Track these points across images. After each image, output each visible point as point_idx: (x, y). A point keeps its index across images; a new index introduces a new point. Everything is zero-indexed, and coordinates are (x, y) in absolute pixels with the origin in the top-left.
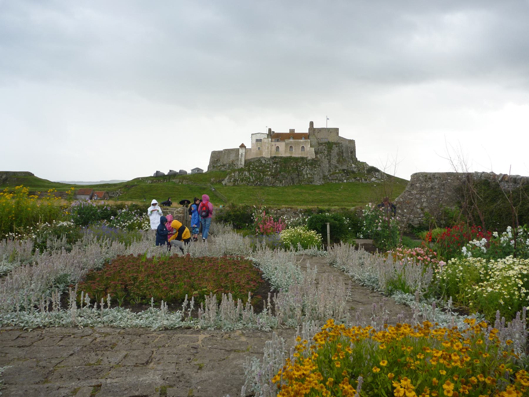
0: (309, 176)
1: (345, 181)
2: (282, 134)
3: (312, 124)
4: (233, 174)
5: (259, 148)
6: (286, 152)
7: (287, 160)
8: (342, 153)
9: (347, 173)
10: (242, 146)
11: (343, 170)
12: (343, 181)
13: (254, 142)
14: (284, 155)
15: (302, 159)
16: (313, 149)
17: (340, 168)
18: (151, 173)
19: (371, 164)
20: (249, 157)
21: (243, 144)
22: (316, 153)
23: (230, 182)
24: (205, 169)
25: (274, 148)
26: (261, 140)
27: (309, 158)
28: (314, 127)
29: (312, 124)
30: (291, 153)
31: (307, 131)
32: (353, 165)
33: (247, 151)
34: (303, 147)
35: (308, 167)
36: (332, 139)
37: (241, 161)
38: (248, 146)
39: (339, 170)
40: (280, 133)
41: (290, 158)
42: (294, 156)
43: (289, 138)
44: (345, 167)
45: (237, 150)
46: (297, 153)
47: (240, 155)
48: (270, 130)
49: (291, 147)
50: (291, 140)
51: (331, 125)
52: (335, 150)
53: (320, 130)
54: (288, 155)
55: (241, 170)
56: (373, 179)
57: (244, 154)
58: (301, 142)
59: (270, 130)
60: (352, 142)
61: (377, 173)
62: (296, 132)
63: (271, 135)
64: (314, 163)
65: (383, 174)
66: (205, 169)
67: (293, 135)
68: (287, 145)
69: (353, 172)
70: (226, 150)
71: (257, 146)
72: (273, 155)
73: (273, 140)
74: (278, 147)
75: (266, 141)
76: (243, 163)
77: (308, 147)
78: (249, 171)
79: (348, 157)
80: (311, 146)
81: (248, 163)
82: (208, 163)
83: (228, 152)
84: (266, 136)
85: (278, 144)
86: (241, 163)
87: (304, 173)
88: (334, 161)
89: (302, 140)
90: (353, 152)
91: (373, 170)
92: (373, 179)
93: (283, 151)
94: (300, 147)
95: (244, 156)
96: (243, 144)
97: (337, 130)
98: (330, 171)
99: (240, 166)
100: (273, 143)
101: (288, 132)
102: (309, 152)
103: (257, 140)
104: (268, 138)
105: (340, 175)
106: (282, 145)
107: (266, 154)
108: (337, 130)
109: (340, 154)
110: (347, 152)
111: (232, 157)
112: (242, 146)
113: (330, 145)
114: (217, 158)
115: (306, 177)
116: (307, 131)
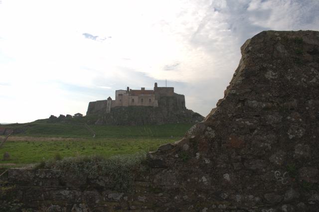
1: (178, 122)
3: (156, 84)
10: (109, 99)
11: (177, 115)
13: (117, 96)
14: (137, 105)
15: (150, 107)
16: (157, 101)
18: (47, 117)
22: (159, 103)
24: (84, 114)
25: (131, 100)
28: (158, 86)
29: (156, 84)
32: (183, 112)
38: (114, 98)
42: (143, 105)
45: (104, 102)
46: (146, 104)
47: (108, 105)
48: (128, 88)
49: (142, 100)
54: (140, 104)
57: (110, 104)
59: (128, 88)
60: (183, 96)
61: (199, 117)
62: (146, 89)
66: (84, 114)
74: (133, 100)
76: (110, 109)
77: (153, 100)
82: (86, 110)
84: (125, 92)
85: (133, 97)
90: (183, 102)
93: (137, 102)
97: (172, 89)
99: (108, 112)
100: (130, 97)
101: (140, 89)
102: (155, 104)
103: (119, 95)
104: (127, 93)
106: (136, 98)
107: (125, 104)
108: (172, 89)
112: (109, 99)
114: (92, 105)
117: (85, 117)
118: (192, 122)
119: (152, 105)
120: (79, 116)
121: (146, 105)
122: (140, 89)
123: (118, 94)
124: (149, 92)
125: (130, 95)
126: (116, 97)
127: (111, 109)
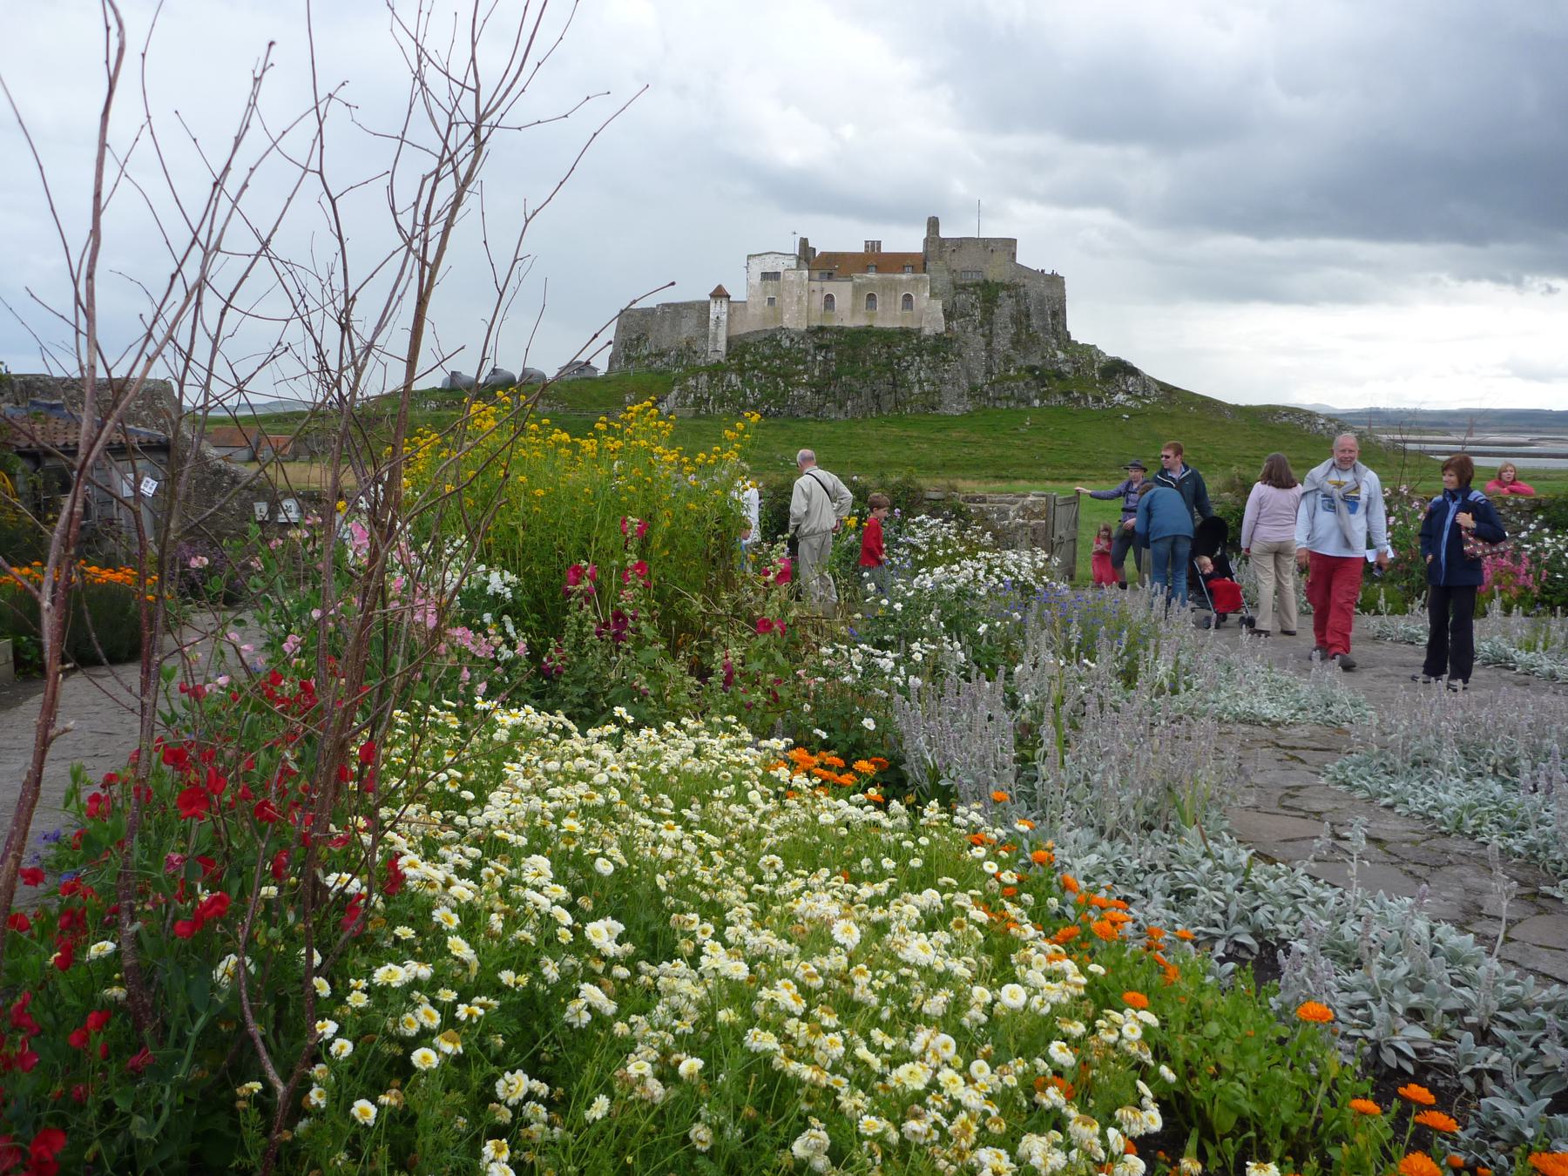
0: (926, 387)
1: (1037, 403)
2: (843, 254)
4: (692, 382)
5: (771, 301)
6: (854, 311)
7: (858, 339)
8: (1028, 316)
9: (1043, 377)
10: (719, 294)
11: (1031, 370)
12: (1028, 402)
13: (756, 279)
14: (849, 323)
15: (906, 333)
16: (938, 305)
17: (1021, 362)
19: (1111, 348)
20: (741, 329)
21: (720, 287)
22: (949, 316)
23: (684, 405)
24: (601, 365)
25: (818, 301)
26: (775, 276)
27: (927, 331)
28: (943, 234)
29: (933, 224)
30: (871, 317)
31: (918, 247)
32: (1060, 355)
33: (735, 308)
34: (908, 298)
35: (922, 361)
36: (994, 273)
37: (715, 340)
38: (738, 293)
39: (1019, 370)
40: (836, 254)
41: (868, 332)
43: (866, 269)
44: (1035, 361)
45: (704, 308)
46: (889, 317)
47: (711, 324)
48: (804, 242)
49: (871, 297)
50: (872, 275)
51: (993, 230)
52: (1006, 308)
53: (960, 243)
54: (860, 321)
55: (715, 370)
56: (1120, 397)
57: (724, 317)
58: (901, 281)
59: (804, 242)
60: (1056, 281)
61: (1131, 379)
63: (807, 261)
64: (941, 347)
65: (1146, 383)
66: (601, 365)
67: (874, 259)
68: (857, 290)
69: (1060, 375)
70: (668, 305)
71: (766, 293)
72: (816, 324)
73: (816, 275)
74: (829, 298)
75: (792, 276)
76: (722, 346)
77: (923, 298)
78: (741, 371)
79: (1044, 328)
80: (933, 295)
81: (737, 347)
83: (676, 311)
84: (793, 264)
85: (830, 287)
86: (718, 348)
87: (911, 377)
88: (1002, 343)
89: (904, 277)
90: (1059, 314)
91: (1119, 370)
92: (1120, 397)
93: (848, 313)
94: (900, 298)
95: (723, 325)
96: (720, 287)
97: (1012, 243)
98: (989, 372)
99: (713, 358)
100: (816, 285)
101: (862, 250)
102: (929, 315)
103: (765, 276)
104: (798, 268)
105: (1022, 384)
106: (843, 292)
107: (794, 319)
109: (1021, 318)
110: (1042, 312)
111: (688, 327)
112: (719, 294)
113: (989, 293)
114: (636, 328)
115: (916, 390)
116: (918, 247)
117: (605, 380)
118: (1098, 400)
119: (912, 325)
120: (579, 370)
121: (888, 324)
122: (862, 250)
123: (758, 268)
124: (899, 262)
125: (816, 275)
126: (750, 286)
127: (729, 341)
